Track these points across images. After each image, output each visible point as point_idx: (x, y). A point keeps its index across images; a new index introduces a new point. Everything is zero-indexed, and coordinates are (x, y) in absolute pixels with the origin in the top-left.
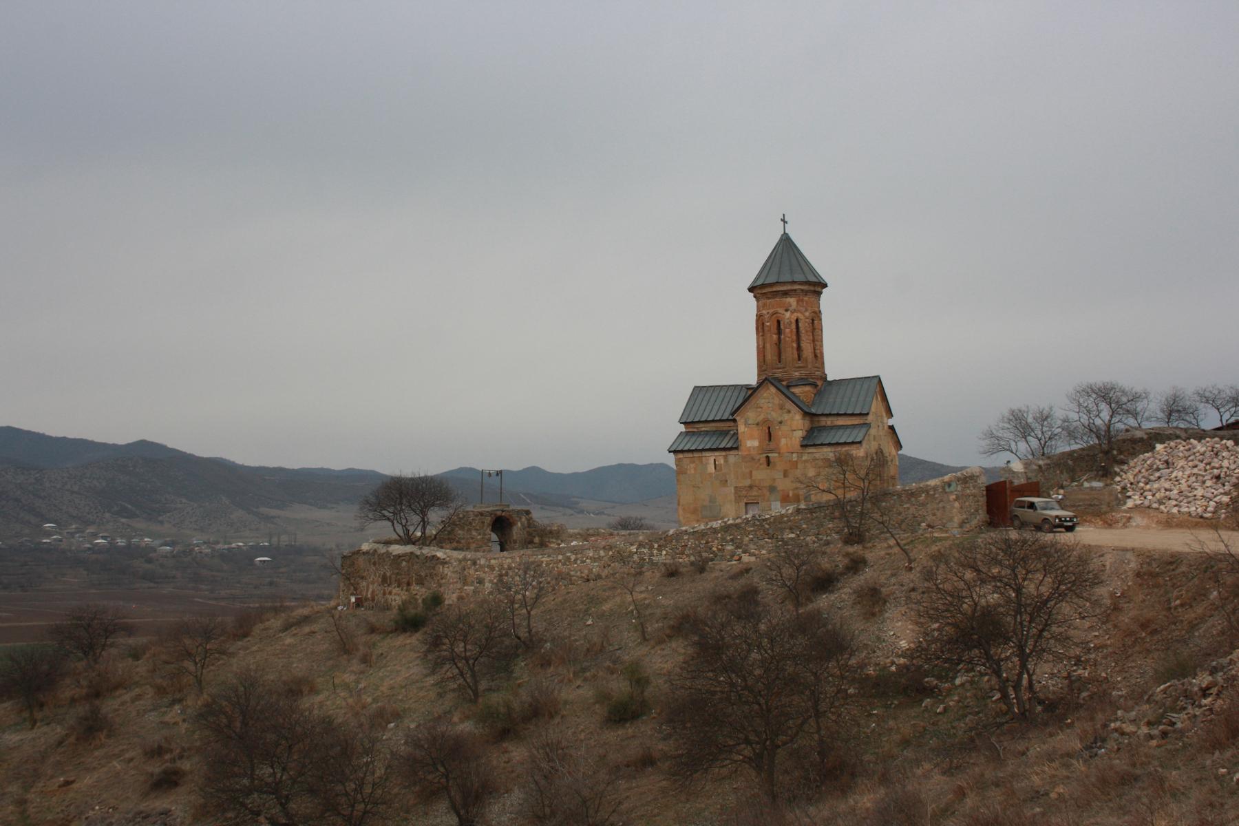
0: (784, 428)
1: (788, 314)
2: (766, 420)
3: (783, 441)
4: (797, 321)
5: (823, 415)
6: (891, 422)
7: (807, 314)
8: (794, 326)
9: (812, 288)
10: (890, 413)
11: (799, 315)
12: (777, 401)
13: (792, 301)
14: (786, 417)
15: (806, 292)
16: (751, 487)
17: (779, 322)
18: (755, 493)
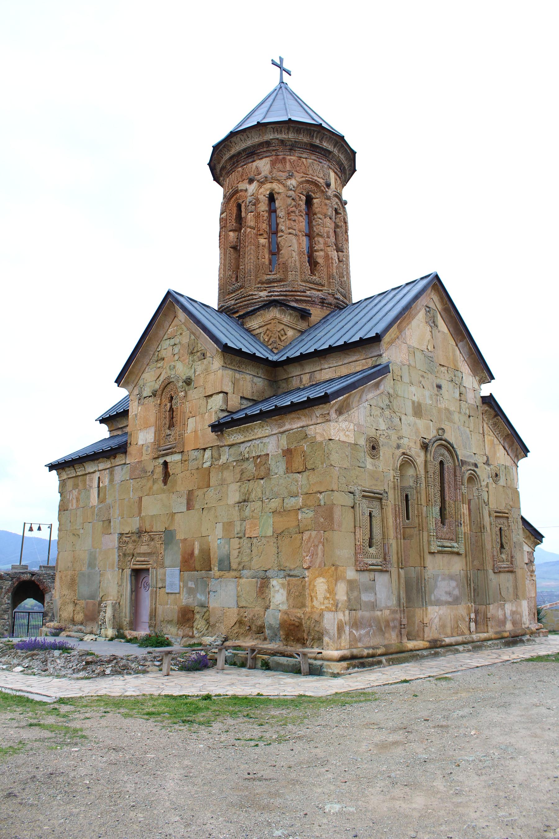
0: (194, 394)
1: (252, 188)
2: (167, 384)
3: (191, 424)
4: (272, 198)
5: (289, 361)
6: (486, 390)
7: (292, 182)
8: (263, 207)
9: (304, 138)
10: (484, 372)
11: (276, 187)
12: (185, 339)
13: (263, 165)
14: (199, 367)
15: (293, 147)
16: (140, 533)
17: (239, 206)
18: (144, 549)
